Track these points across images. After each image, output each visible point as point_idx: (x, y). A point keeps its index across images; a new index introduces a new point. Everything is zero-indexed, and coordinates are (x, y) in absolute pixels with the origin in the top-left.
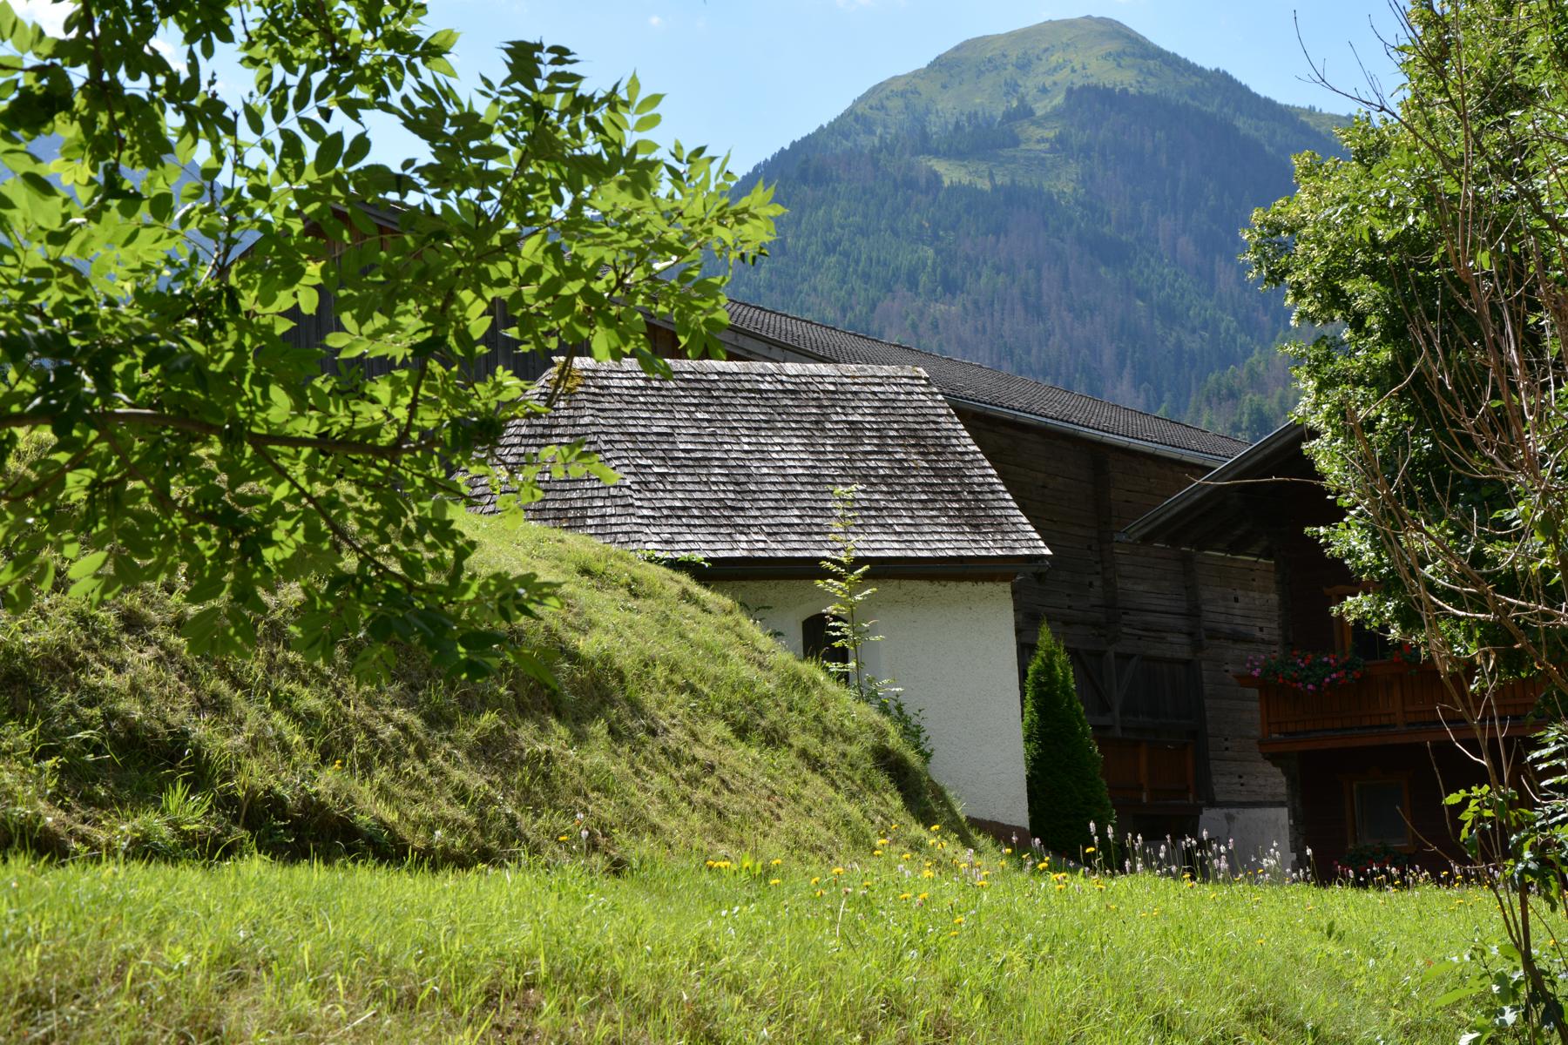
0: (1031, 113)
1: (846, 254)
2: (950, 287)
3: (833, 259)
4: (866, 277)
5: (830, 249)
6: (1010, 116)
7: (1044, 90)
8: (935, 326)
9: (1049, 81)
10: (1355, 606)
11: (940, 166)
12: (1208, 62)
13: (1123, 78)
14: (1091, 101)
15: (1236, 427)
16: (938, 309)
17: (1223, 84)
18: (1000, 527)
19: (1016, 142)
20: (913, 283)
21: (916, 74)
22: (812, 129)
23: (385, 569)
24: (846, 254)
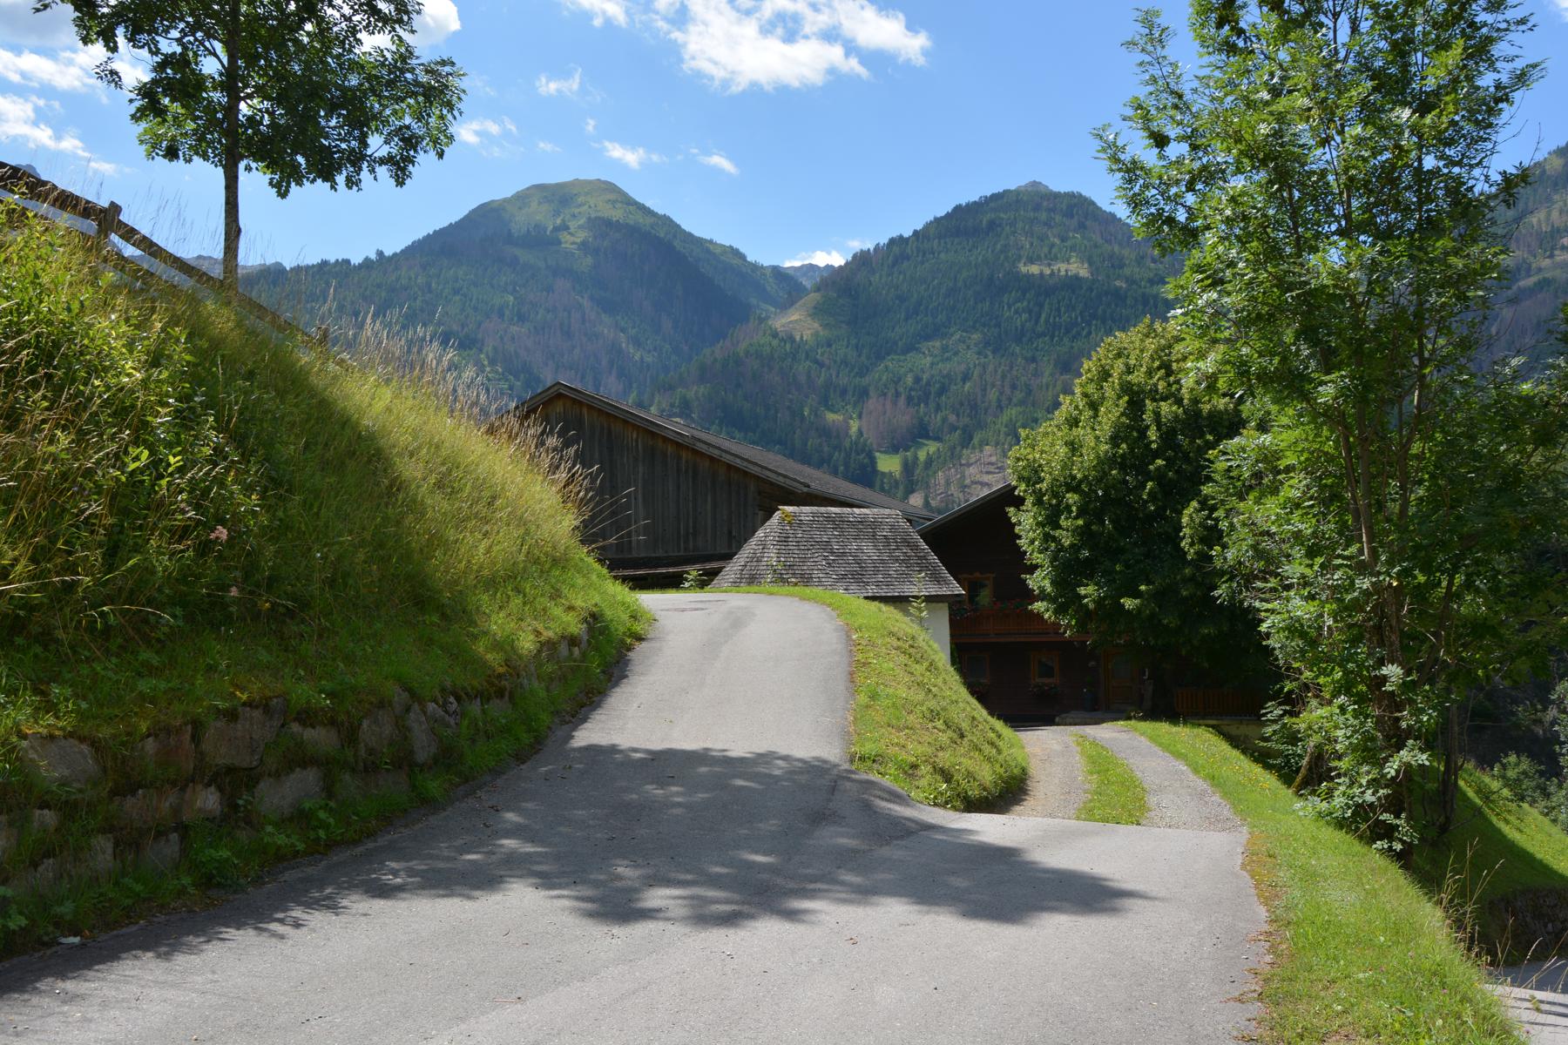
0: (567, 228)
1: (465, 296)
2: (522, 318)
3: (457, 298)
4: (476, 309)
5: (456, 292)
6: (556, 229)
7: (574, 216)
8: (513, 338)
9: (576, 211)
10: (1039, 606)
11: (518, 252)
12: (661, 212)
13: (617, 214)
14: (602, 226)
15: (672, 405)
16: (514, 329)
17: (667, 221)
18: (947, 583)
19: (560, 243)
20: (501, 315)
21: (505, 200)
22: (708, 237)
23: (770, 776)
24: (465, 296)
